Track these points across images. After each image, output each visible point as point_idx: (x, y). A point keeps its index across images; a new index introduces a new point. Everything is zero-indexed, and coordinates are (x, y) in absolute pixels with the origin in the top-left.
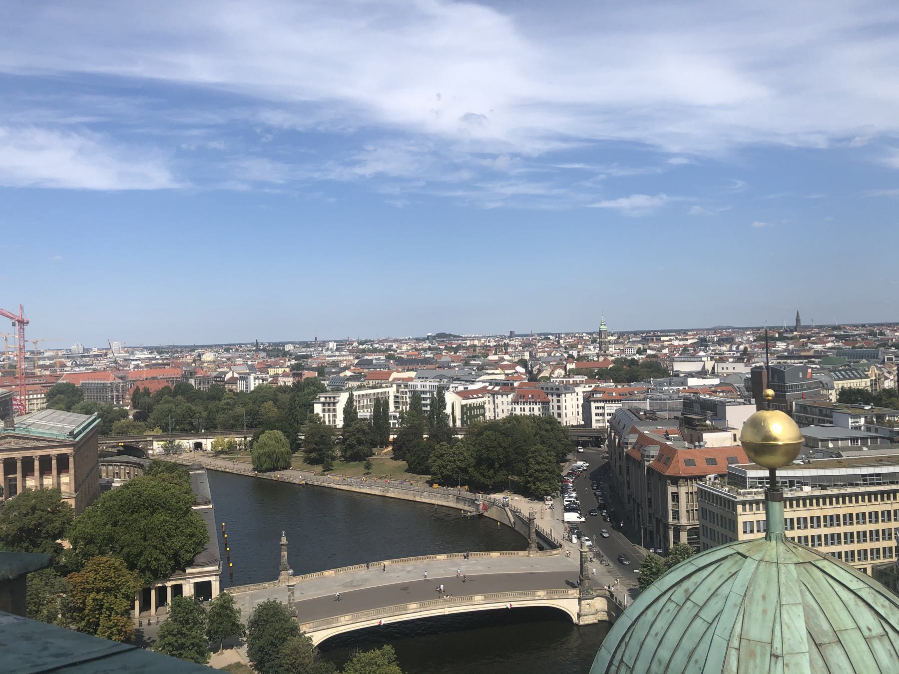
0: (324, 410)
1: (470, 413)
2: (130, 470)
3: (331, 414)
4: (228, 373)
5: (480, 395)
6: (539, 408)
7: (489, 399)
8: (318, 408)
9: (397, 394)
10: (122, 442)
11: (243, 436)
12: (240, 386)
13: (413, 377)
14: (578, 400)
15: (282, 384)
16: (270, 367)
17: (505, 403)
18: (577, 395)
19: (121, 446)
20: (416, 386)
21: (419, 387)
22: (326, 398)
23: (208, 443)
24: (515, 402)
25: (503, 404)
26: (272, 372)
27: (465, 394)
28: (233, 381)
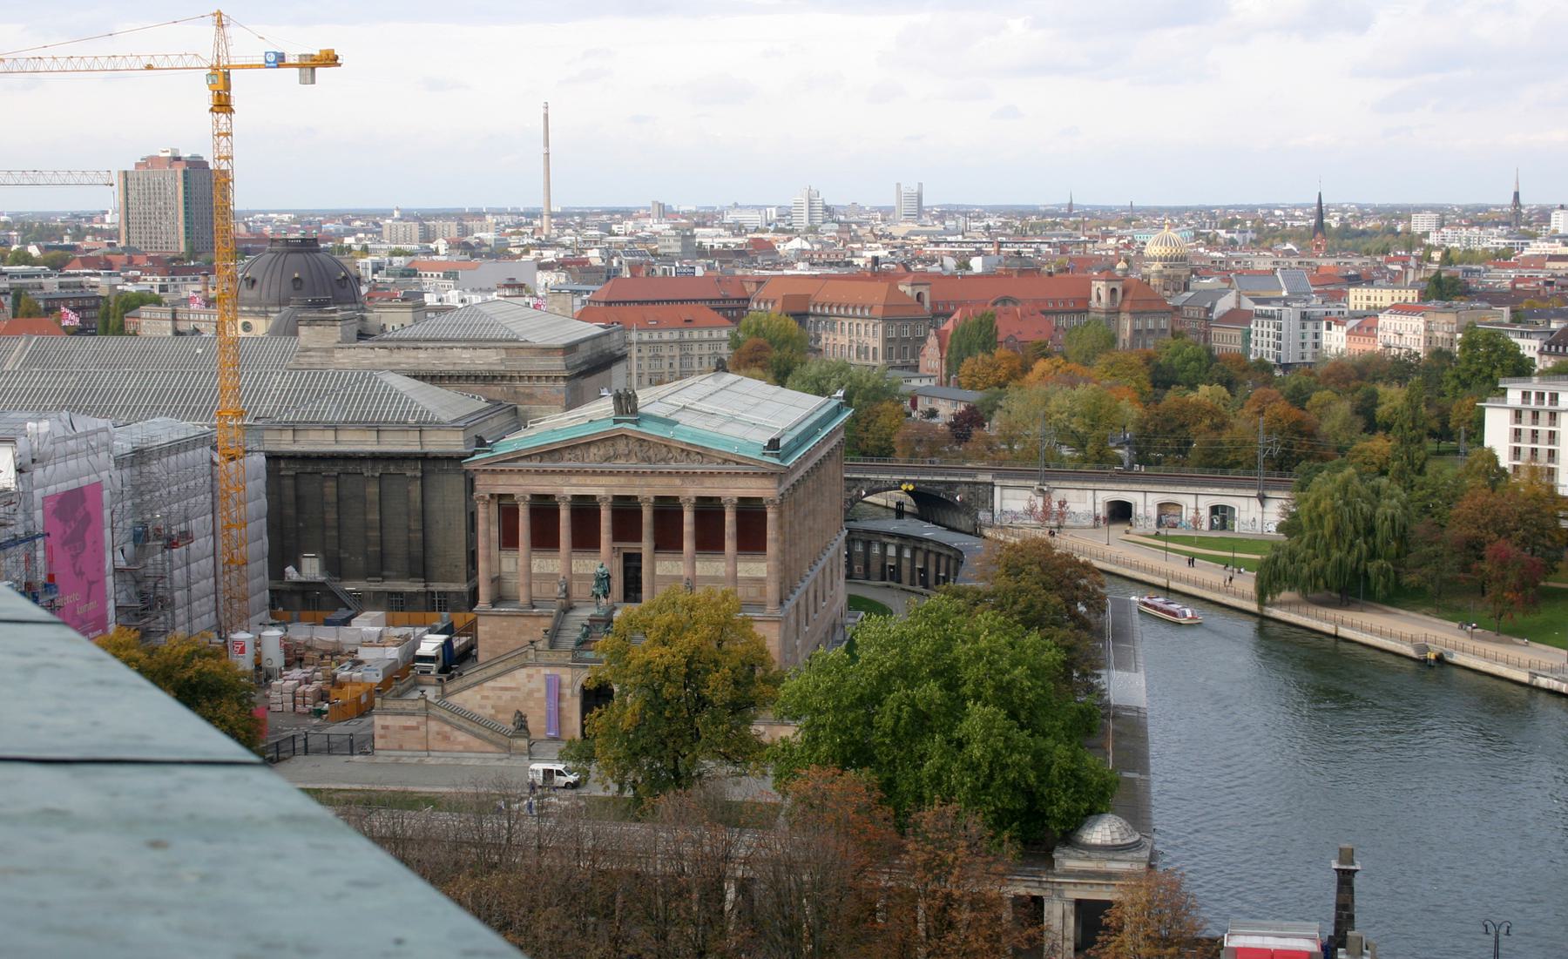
0: (1517, 433)
2: (926, 562)
8: (1498, 430)
10: (910, 482)
11: (1255, 493)
16: (1356, 280)
19: (907, 491)
22: (1526, 395)
23: (1145, 502)
26: (1358, 298)
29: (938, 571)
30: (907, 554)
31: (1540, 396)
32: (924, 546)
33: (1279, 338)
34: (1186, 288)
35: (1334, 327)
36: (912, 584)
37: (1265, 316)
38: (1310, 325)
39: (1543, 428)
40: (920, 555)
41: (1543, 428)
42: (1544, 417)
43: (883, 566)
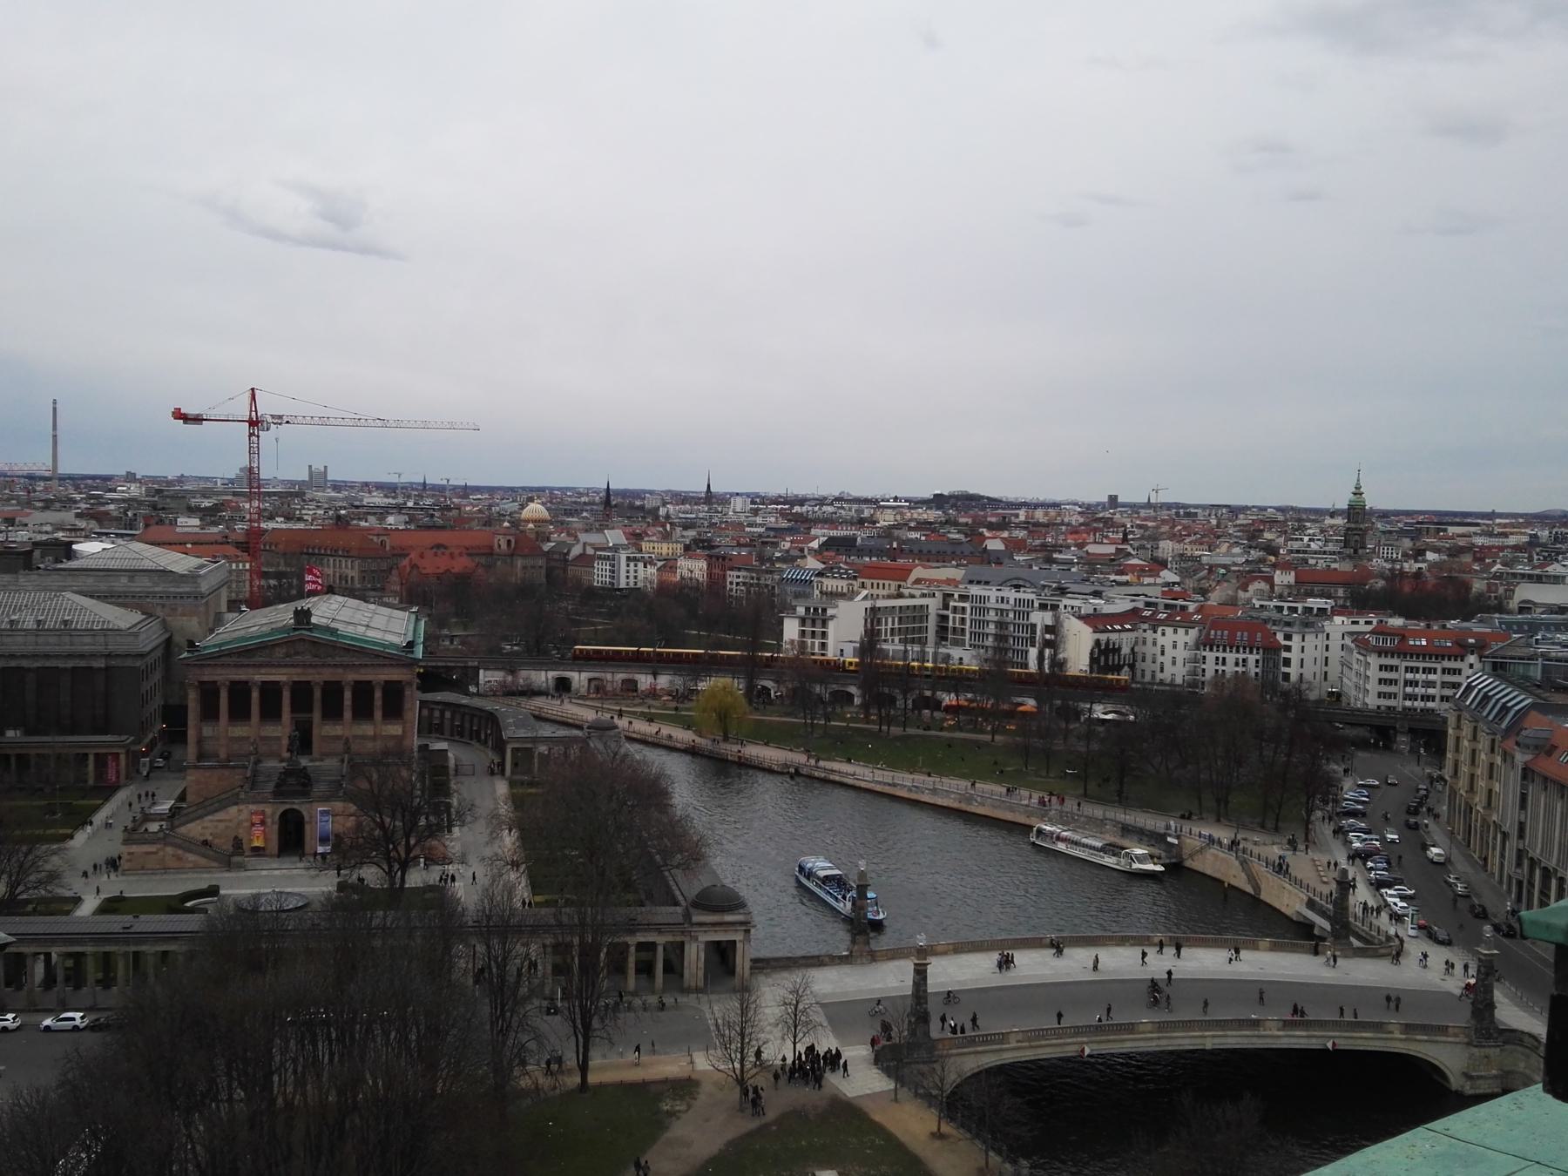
0: (803, 631)
1: (1107, 660)
2: (463, 720)
3: (817, 642)
4: (573, 545)
5: (1128, 626)
6: (1257, 661)
7: (1145, 635)
8: (791, 629)
9: (945, 612)
12: (600, 575)
13: (959, 578)
14: (1327, 650)
15: (686, 574)
17: (1180, 645)
18: (1328, 638)
20: (985, 599)
21: (993, 600)
22: (808, 609)
23: (579, 678)
24: (1205, 643)
25: (1175, 647)
27: (1095, 620)
28: (585, 560)
29: (472, 727)
30: (448, 715)
31: (816, 610)
32: (462, 710)
33: (613, 572)
34: (549, 540)
35: (649, 566)
36: (452, 735)
37: (600, 558)
38: (632, 564)
39: (818, 629)
40: (458, 717)
41: (818, 629)
42: (819, 623)
43: (431, 724)
